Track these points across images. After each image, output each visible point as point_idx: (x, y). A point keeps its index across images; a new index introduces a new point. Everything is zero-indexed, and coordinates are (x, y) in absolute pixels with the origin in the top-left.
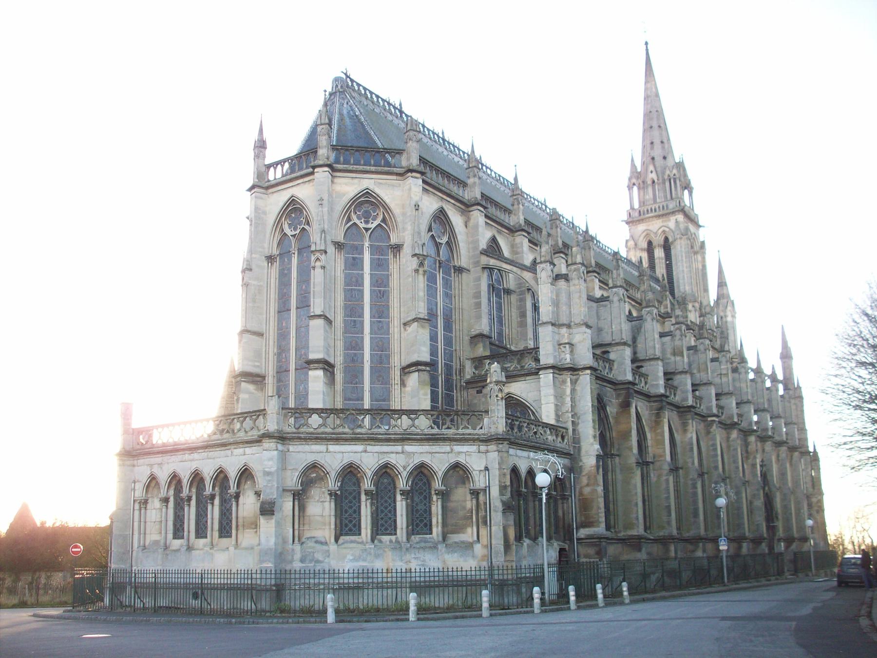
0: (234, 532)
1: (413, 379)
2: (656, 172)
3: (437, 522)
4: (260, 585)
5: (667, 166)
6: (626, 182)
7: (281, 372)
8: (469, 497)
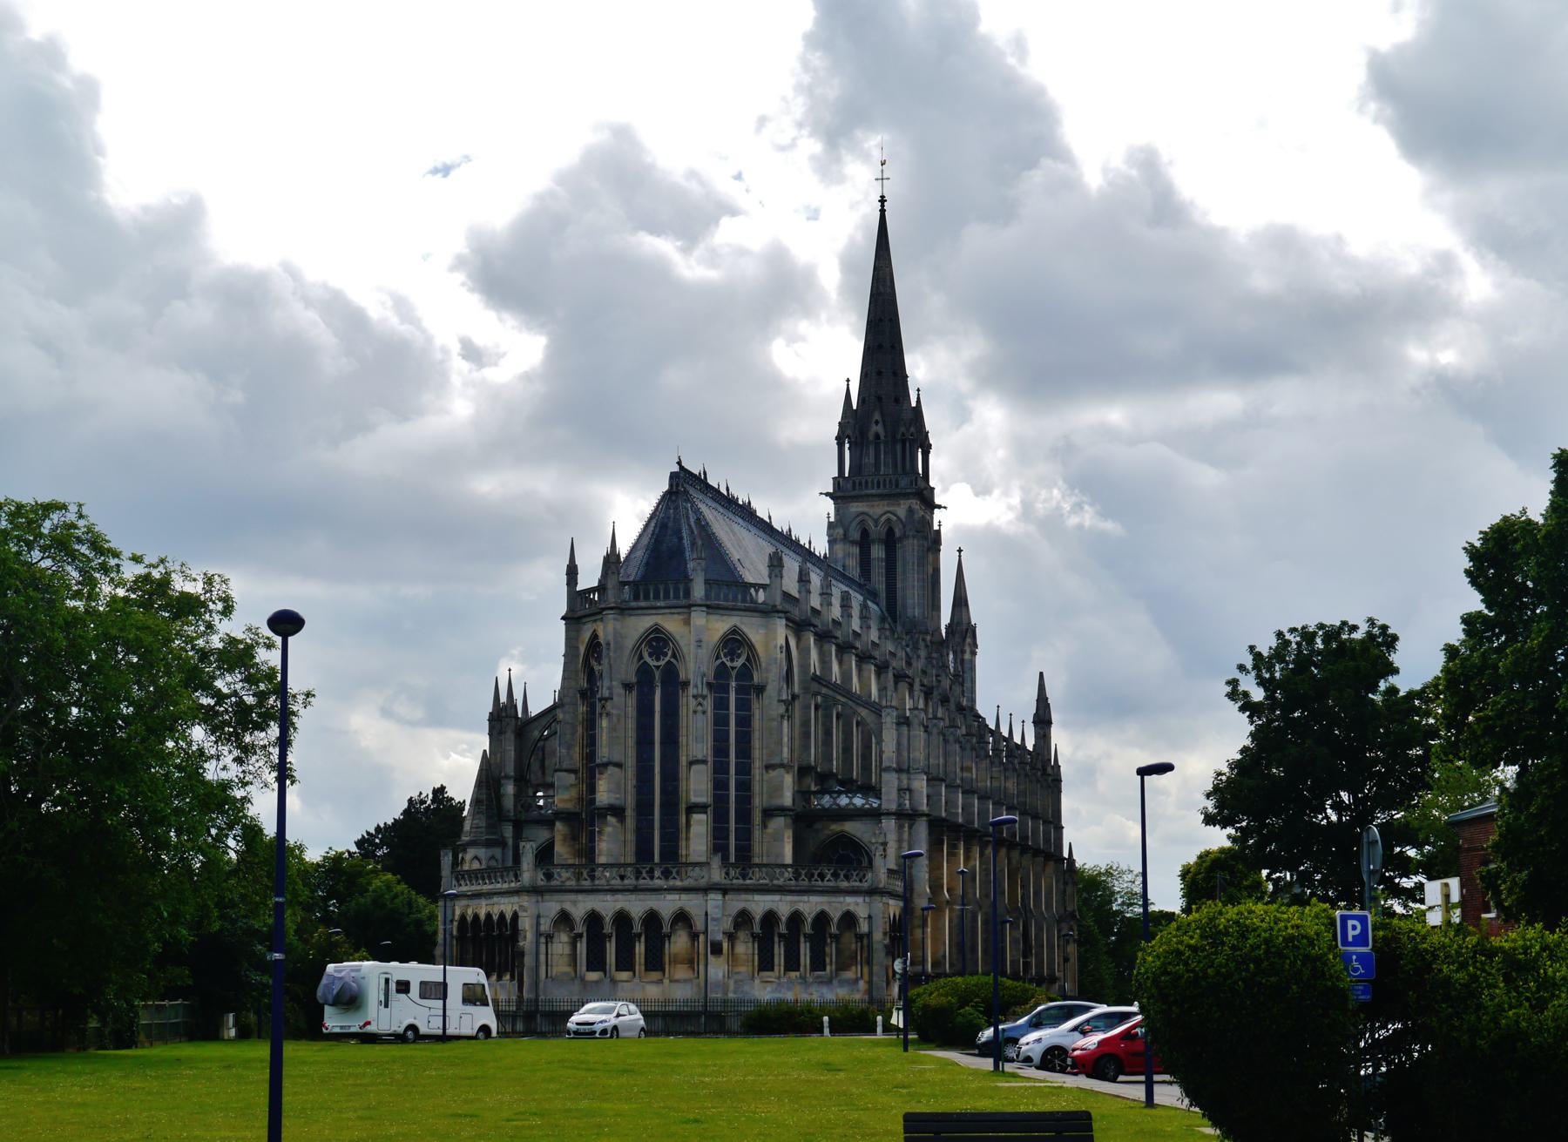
0: (667, 966)
1: (778, 823)
2: (884, 422)
3: (831, 961)
4: (651, 1011)
5: (903, 420)
6: (835, 430)
7: (644, 807)
8: (854, 940)
